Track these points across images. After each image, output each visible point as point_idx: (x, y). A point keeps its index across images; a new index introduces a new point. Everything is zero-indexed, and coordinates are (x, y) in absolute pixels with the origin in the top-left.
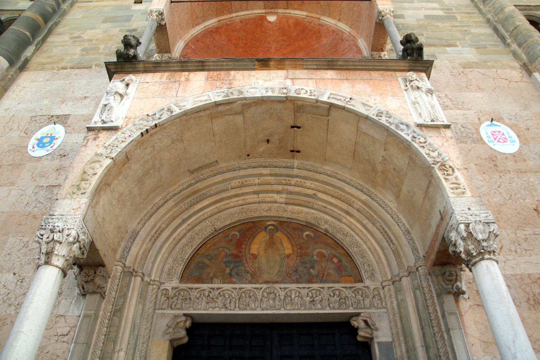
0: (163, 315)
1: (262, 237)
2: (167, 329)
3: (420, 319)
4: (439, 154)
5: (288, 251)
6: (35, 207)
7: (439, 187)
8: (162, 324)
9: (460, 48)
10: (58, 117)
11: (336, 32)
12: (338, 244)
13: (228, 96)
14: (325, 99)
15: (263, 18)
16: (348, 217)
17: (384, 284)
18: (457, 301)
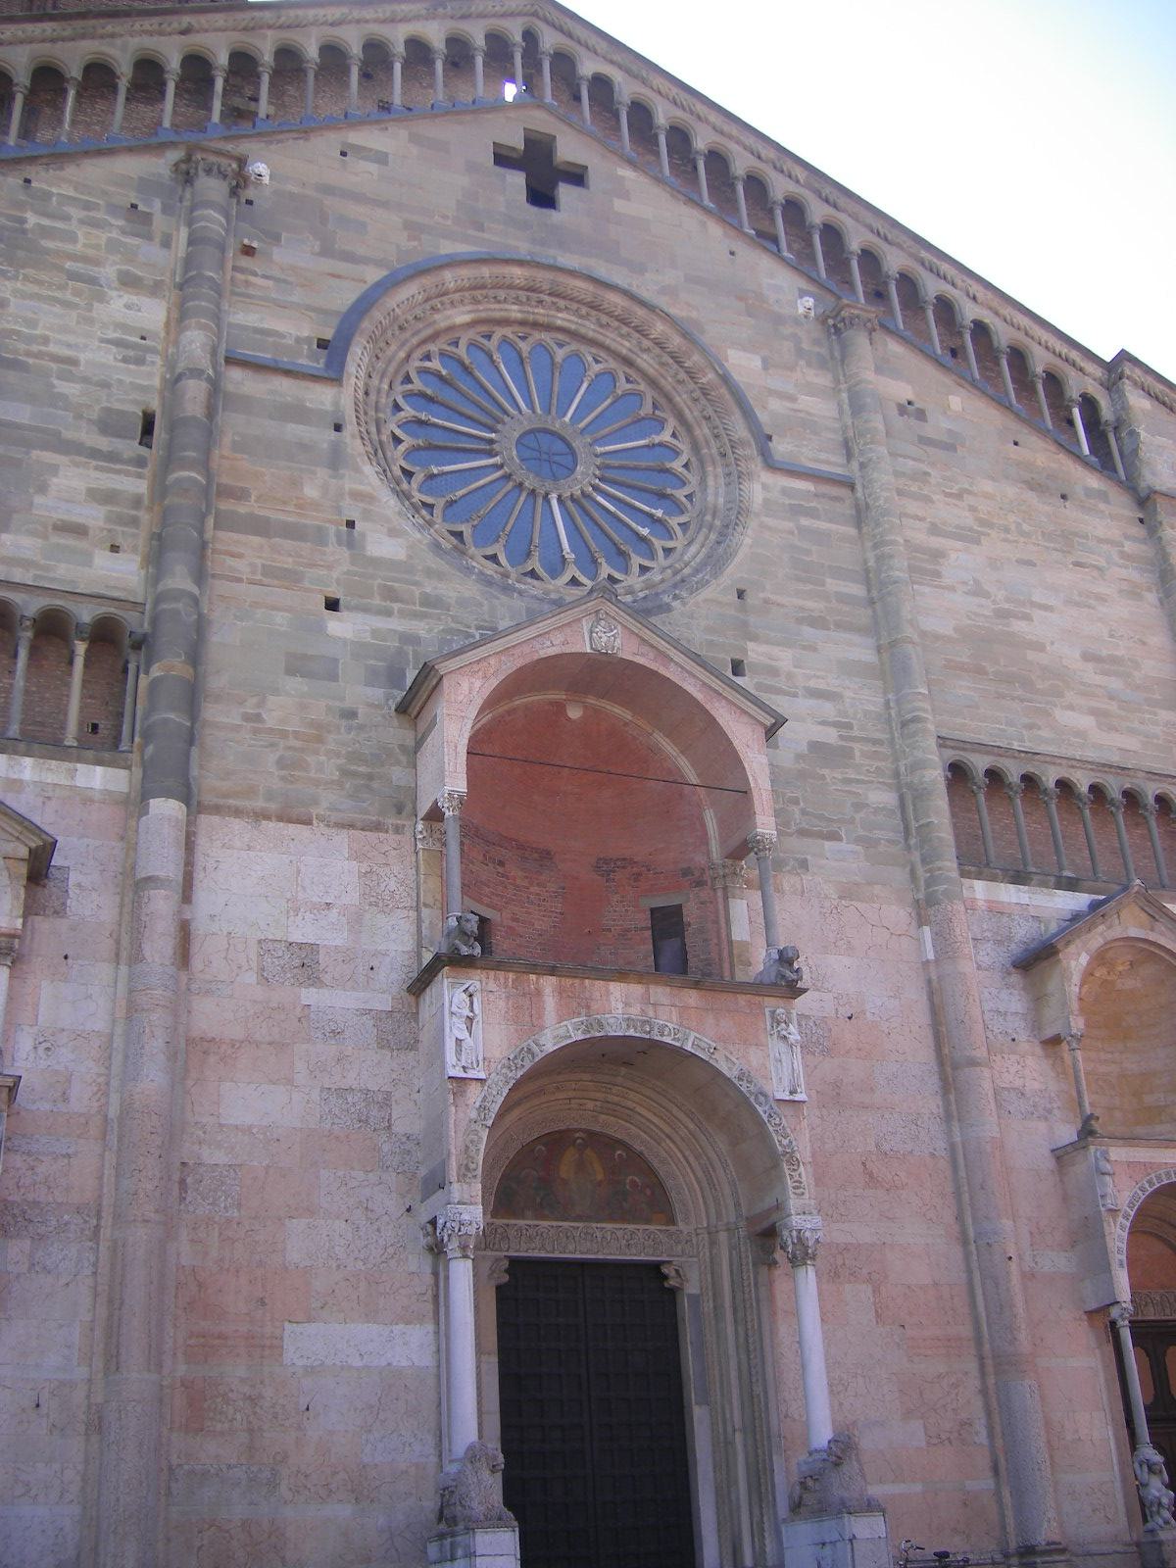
0: (483, 1257)
1: (570, 1156)
2: (491, 1274)
3: (732, 1281)
4: (791, 1142)
5: (600, 1177)
6: (333, 1123)
7: (781, 1178)
8: (486, 1266)
9: (843, 845)
10: (301, 946)
11: (677, 781)
12: (651, 1172)
13: (589, 1032)
14: (688, 1047)
15: (560, 707)
16: (668, 1141)
17: (699, 1231)
18: (769, 1270)
